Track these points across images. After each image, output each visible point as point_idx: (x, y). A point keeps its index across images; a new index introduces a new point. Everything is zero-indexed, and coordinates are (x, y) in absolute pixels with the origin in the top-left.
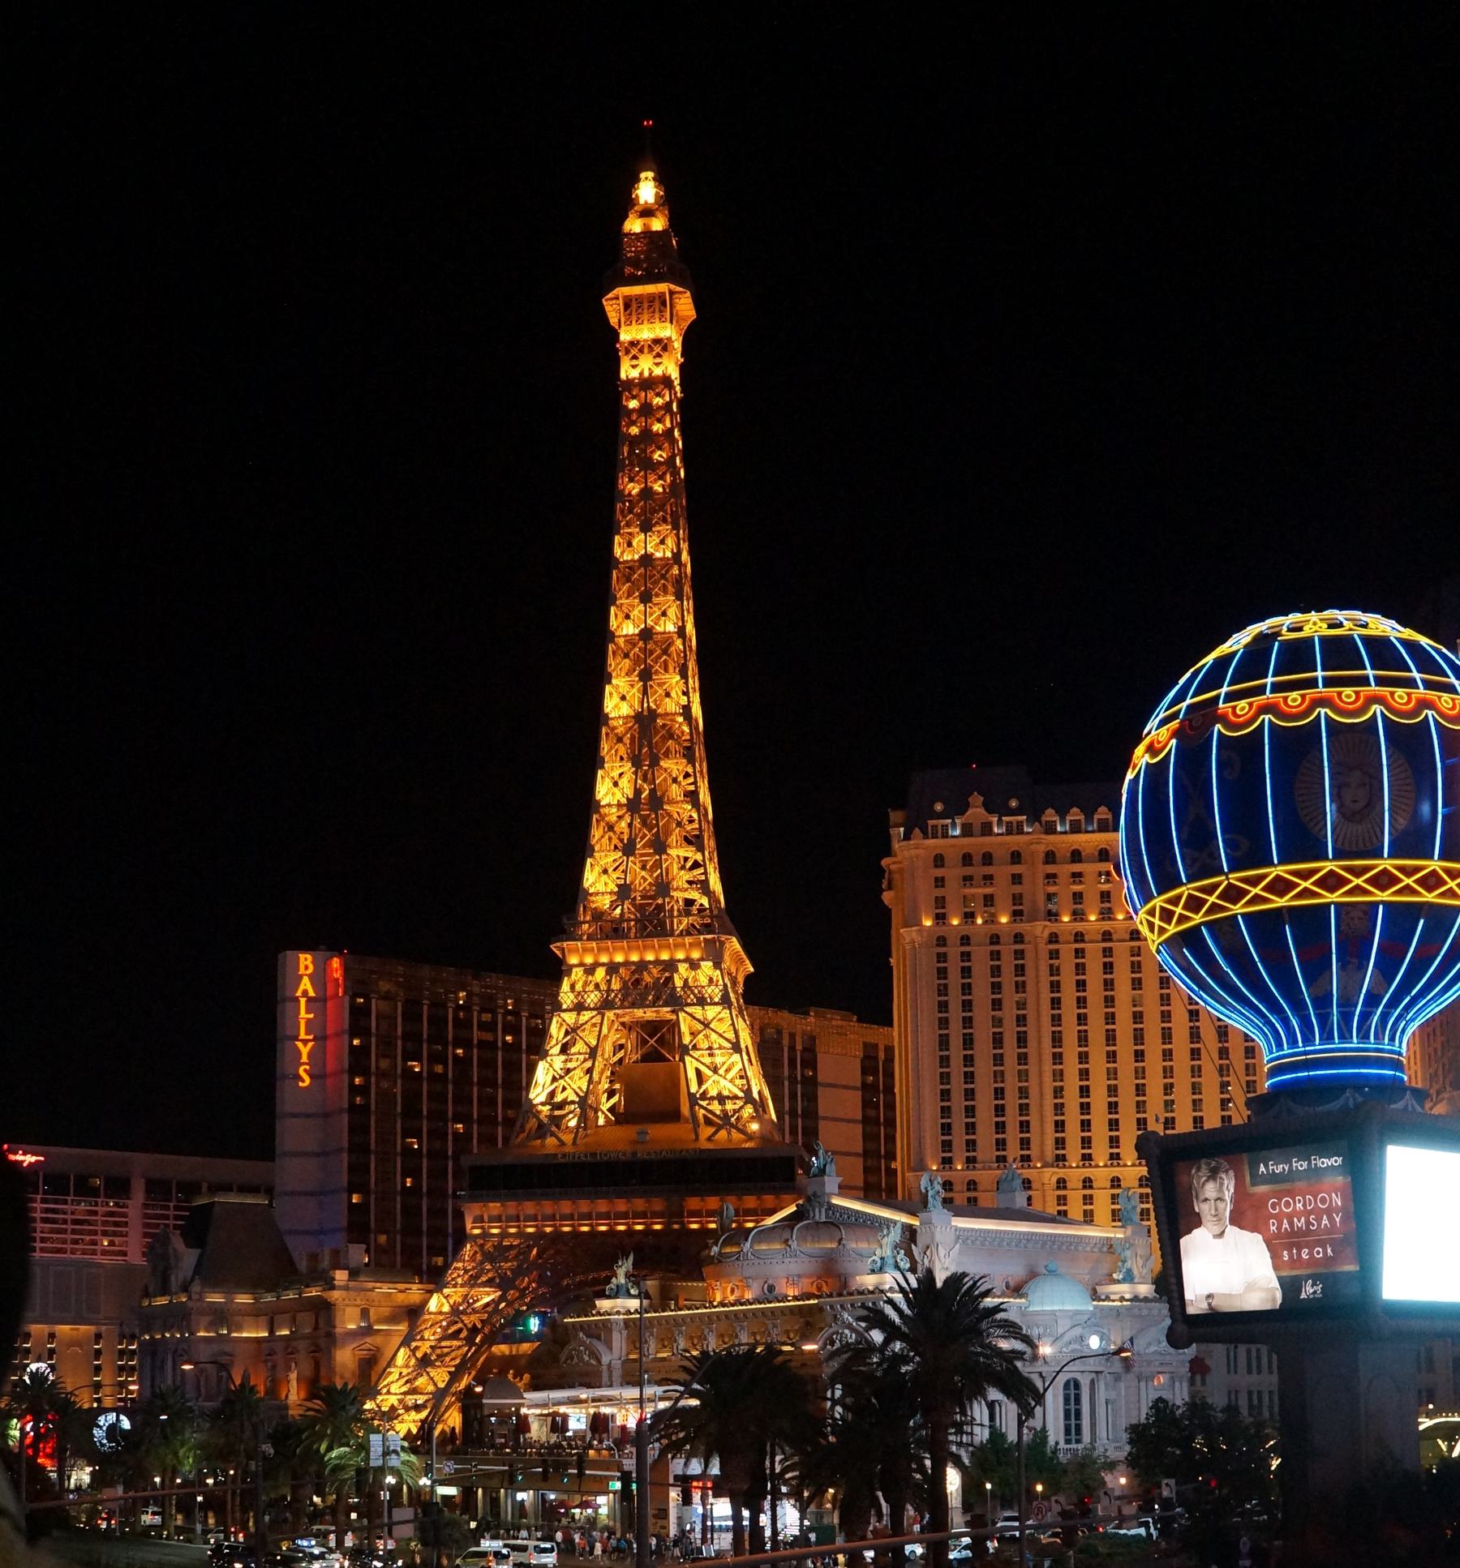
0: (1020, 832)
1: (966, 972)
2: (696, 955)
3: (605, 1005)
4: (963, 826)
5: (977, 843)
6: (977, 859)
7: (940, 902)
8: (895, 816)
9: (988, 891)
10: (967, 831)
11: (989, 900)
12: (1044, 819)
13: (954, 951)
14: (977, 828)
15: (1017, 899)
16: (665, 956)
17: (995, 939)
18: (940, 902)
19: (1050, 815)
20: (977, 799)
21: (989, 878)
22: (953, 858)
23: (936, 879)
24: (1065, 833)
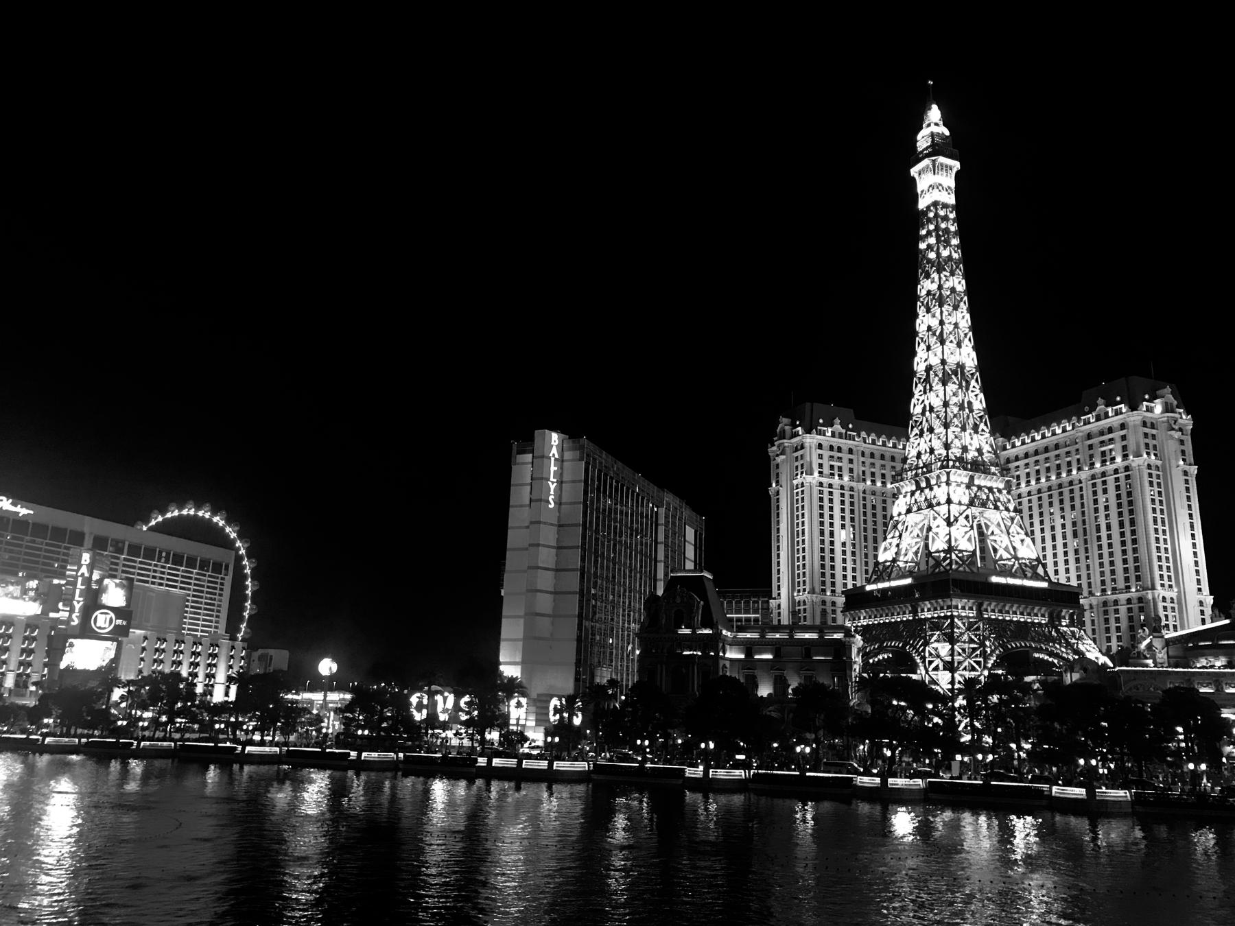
1: (831, 501)
2: (1001, 486)
3: (971, 503)
5: (836, 442)
7: (821, 466)
8: (784, 422)
10: (833, 435)
11: (840, 468)
13: (826, 490)
15: (851, 470)
16: (989, 484)
17: (842, 487)
18: (821, 466)
19: (863, 434)
20: (837, 421)
21: (840, 459)
22: (825, 445)
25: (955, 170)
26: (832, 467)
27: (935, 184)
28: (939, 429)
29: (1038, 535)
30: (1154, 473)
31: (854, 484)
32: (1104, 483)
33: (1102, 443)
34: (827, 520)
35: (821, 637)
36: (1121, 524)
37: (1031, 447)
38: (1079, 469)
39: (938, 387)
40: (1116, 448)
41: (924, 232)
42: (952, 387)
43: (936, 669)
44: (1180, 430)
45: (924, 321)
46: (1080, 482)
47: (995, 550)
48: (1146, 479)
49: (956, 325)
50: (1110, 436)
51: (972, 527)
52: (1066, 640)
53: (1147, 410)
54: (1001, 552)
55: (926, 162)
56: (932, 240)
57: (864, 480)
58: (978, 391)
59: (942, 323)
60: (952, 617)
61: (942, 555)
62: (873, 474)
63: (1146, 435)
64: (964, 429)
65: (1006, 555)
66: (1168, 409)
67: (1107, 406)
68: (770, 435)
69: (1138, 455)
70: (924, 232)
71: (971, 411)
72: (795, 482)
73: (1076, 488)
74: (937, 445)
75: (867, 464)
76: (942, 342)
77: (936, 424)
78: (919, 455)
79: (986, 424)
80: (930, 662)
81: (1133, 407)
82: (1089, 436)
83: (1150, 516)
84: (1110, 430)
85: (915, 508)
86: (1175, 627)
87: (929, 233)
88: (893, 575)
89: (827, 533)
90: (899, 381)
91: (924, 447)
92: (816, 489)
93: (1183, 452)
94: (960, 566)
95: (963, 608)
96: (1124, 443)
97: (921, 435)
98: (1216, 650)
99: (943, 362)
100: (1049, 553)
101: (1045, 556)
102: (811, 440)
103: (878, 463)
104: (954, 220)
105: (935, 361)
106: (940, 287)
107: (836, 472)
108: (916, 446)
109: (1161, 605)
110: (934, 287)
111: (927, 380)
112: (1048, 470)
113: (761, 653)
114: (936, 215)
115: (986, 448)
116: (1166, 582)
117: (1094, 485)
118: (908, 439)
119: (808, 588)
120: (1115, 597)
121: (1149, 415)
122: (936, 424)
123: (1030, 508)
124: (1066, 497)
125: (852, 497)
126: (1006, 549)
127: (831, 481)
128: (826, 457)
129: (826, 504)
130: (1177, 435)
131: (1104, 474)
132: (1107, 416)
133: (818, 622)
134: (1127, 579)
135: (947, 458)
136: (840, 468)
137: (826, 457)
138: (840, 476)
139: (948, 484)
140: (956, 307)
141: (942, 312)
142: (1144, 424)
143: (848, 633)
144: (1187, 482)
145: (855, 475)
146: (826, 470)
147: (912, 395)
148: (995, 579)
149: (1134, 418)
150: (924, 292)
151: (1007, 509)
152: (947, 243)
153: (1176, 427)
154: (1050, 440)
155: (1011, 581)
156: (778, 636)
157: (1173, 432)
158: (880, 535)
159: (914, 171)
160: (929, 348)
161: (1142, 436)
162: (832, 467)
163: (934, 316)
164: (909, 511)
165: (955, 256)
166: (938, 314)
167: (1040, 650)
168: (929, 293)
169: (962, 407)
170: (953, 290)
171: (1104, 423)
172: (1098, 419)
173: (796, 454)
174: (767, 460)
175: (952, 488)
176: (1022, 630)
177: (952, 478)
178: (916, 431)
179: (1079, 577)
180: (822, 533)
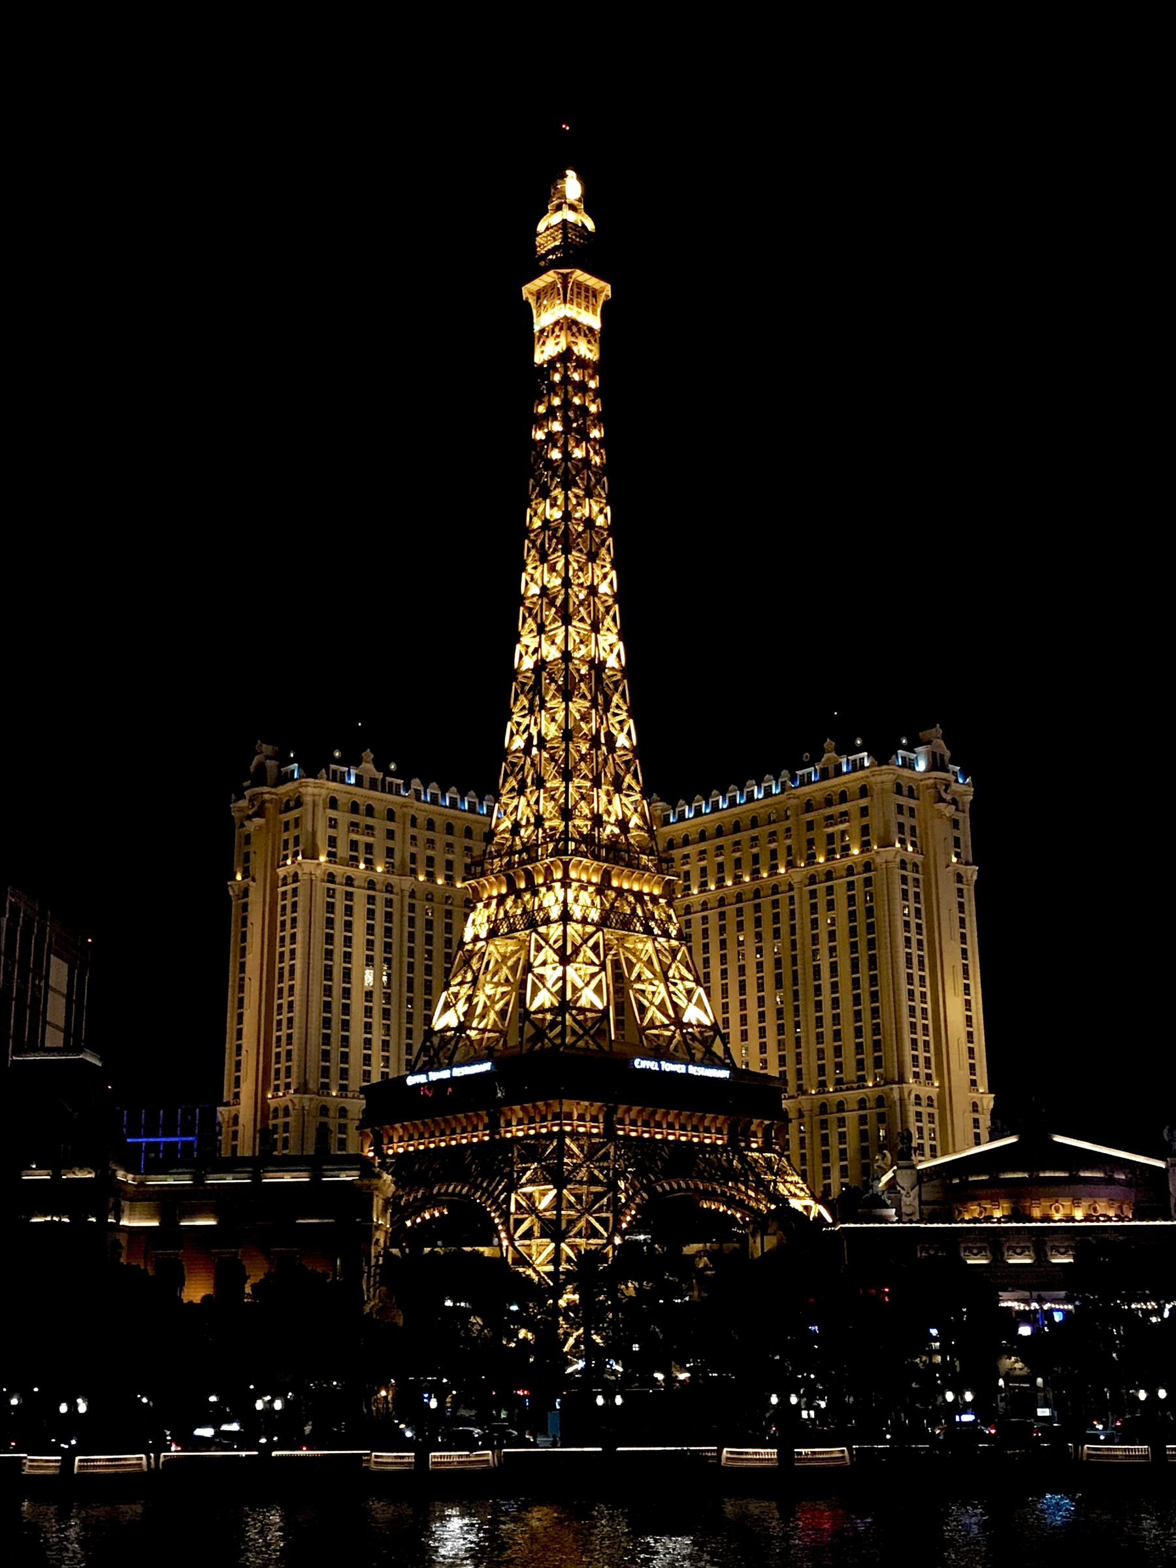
0: (398, 794)
1: (349, 910)
2: (656, 892)
3: (603, 923)
4: (358, 777)
5: (365, 795)
6: (362, 808)
7: (332, 841)
9: (370, 840)
10: (359, 782)
11: (369, 847)
12: (413, 786)
13: (340, 889)
14: (366, 783)
15: (390, 852)
16: (636, 888)
17: (371, 885)
18: (332, 841)
19: (416, 783)
20: (368, 755)
21: (370, 828)
22: (343, 799)
23: (331, 820)
24: (426, 802)
25: (601, 299)
26: (354, 845)
27: (565, 320)
28: (555, 783)
29: (716, 981)
30: (910, 875)
31: (394, 879)
32: (830, 890)
33: (830, 820)
34: (339, 949)
35: (316, 1178)
36: (855, 966)
37: (709, 821)
38: (790, 865)
39: (556, 703)
40: (853, 826)
41: (541, 409)
42: (578, 705)
43: (528, 1235)
44: (954, 802)
45: (536, 579)
46: (791, 888)
47: (643, 1009)
48: (898, 886)
49: (593, 590)
50: (844, 807)
51: (603, 967)
52: (757, 1175)
53: (904, 766)
54: (652, 1012)
55: (550, 277)
56: (557, 427)
57: (414, 872)
58: (624, 716)
59: (566, 583)
60: (562, 1134)
61: (549, 1017)
62: (430, 861)
63: (900, 809)
64: (597, 783)
65: (661, 1018)
66: (936, 764)
67: (840, 753)
68: (237, 775)
69: (886, 843)
70: (541, 409)
71: (612, 749)
72: (281, 872)
73: (783, 898)
74: (548, 808)
75: (421, 842)
76: (567, 621)
77: (549, 770)
78: (516, 828)
79: (635, 776)
80: (518, 1223)
81: (882, 758)
82: (809, 807)
83: (902, 951)
84: (843, 797)
85: (504, 929)
86: (933, 1148)
87: (551, 412)
88: (456, 1058)
89: (337, 973)
90: (491, 685)
91: (524, 813)
92: (321, 887)
93: (957, 841)
94: (580, 1037)
95: (581, 1117)
96: (865, 821)
97: (521, 791)
98: (995, 1190)
99: (566, 656)
100: (734, 1016)
101: (726, 1021)
102: (316, 789)
103: (441, 838)
104: (598, 393)
105: (551, 653)
106: (567, 516)
107: (361, 854)
108: (513, 811)
109: (912, 1109)
110: (557, 514)
111: (536, 688)
112: (738, 863)
113: (192, 1215)
114: (566, 379)
115: (635, 820)
116: (922, 1071)
117: (813, 894)
118: (497, 797)
119: (294, 1080)
120: (839, 1096)
121: (906, 772)
122: (549, 770)
123: (705, 933)
124: (767, 914)
125: (389, 903)
126: (661, 1007)
127: (350, 871)
128: (343, 826)
129: (339, 917)
130: (949, 810)
131: (829, 876)
132: (838, 772)
133: (310, 1151)
134: (860, 1064)
135: (566, 836)
136: (369, 847)
137: (343, 826)
138: (368, 862)
139: (566, 883)
140: (592, 557)
141: (567, 564)
142: (899, 790)
143: (365, 1168)
144: (960, 892)
145: (397, 860)
146: (343, 850)
147: (509, 715)
148: (640, 1064)
149: (884, 777)
150: (537, 523)
151: (666, 934)
152: (583, 436)
153: (948, 798)
154: (744, 810)
155: (667, 1067)
156: (229, 1180)
157: (942, 805)
158: (437, 979)
159: (528, 290)
160: (541, 629)
161: (894, 808)
162: (354, 845)
163: (552, 569)
164: (493, 934)
165: (596, 460)
166: (560, 566)
167: (712, 1196)
168: (546, 523)
169: (595, 742)
170: (589, 522)
171: (834, 784)
172: (824, 775)
173: (285, 817)
174: (227, 826)
175: (571, 894)
176: (683, 1158)
177: (573, 874)
178: (513, 783)
179: (782, 1060)
180: (328, 972)
